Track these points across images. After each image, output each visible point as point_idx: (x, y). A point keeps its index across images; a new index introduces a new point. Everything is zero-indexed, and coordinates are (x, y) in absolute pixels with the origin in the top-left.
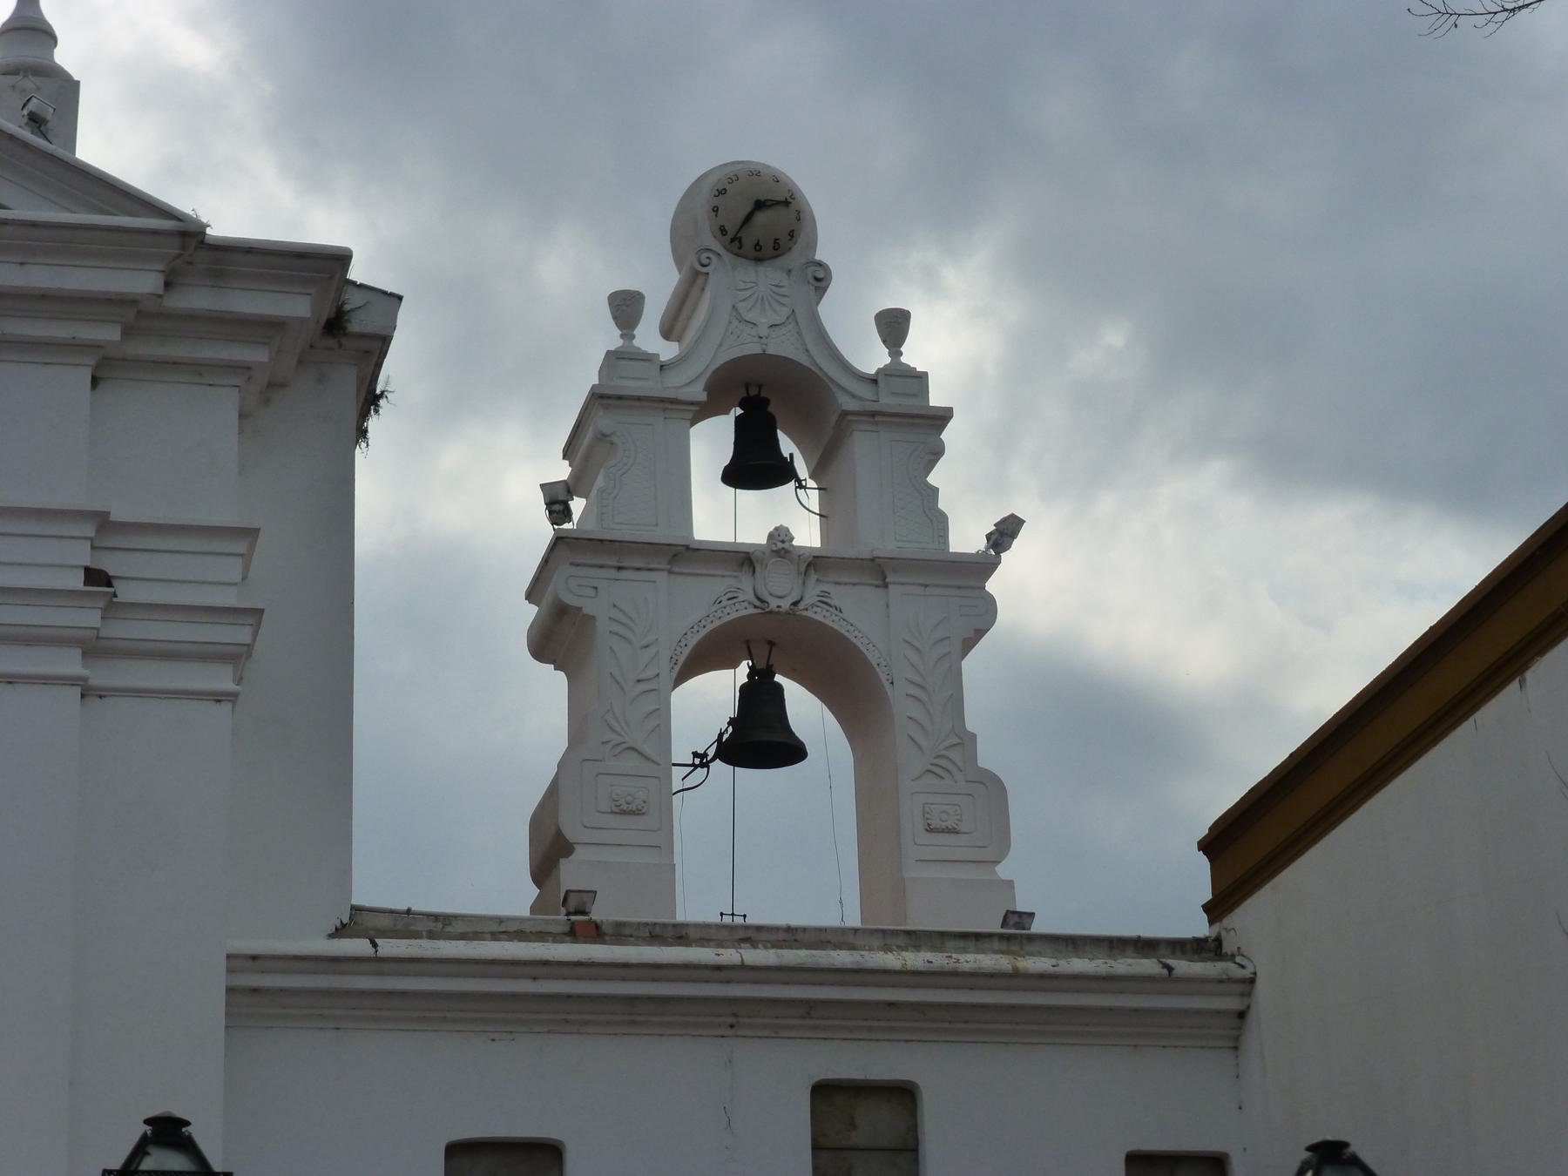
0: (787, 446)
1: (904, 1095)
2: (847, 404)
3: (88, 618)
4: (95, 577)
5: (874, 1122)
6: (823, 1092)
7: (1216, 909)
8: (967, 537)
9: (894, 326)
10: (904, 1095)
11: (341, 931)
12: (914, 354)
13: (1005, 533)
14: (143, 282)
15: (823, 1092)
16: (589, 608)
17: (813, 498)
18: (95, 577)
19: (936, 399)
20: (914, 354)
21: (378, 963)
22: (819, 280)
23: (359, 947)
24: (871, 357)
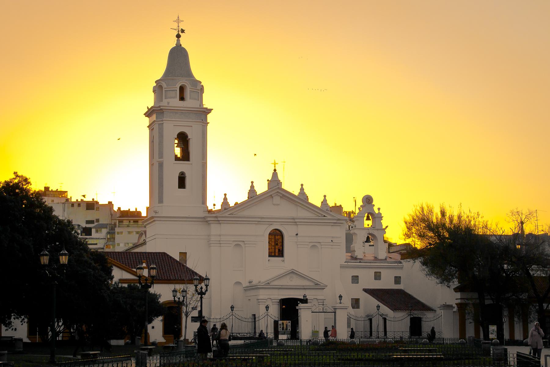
0: (370, 217)
1: (380, 272)
2: (376, 216)
3: (332, 244)
4: (332, 241)
5: (378, 274)
6: (375, 272)
7: (401, 259)
8: (384, 227)
9: (379, 209)
10: (380, 272)
11: (345, 262)
12: (380, 211)
13: (387, 227)
14: (335, 221)
15: (375, 272)
16: (357, 233)
17: (371, 221)
18: (332, 241)
19: (382, 216)
20: (380, 211)
21: (348, 265)
22: (374, 205)
23: (346, 264)
24: (377, 212)
